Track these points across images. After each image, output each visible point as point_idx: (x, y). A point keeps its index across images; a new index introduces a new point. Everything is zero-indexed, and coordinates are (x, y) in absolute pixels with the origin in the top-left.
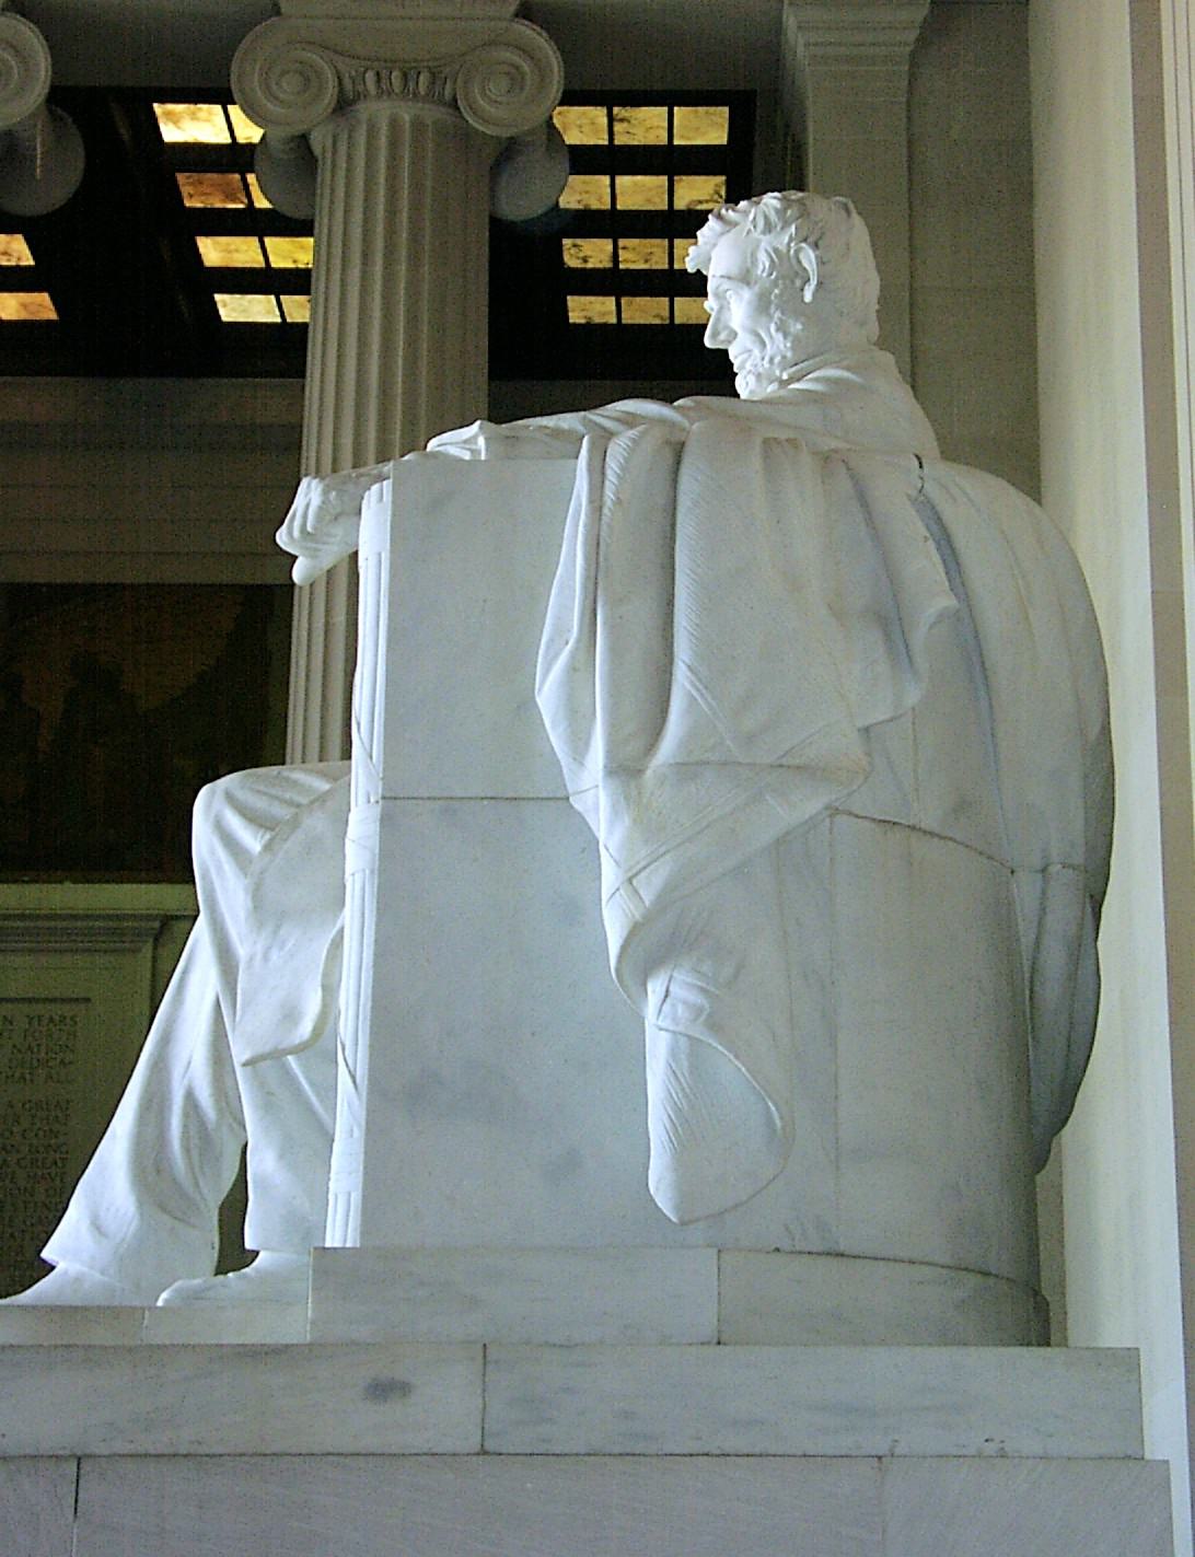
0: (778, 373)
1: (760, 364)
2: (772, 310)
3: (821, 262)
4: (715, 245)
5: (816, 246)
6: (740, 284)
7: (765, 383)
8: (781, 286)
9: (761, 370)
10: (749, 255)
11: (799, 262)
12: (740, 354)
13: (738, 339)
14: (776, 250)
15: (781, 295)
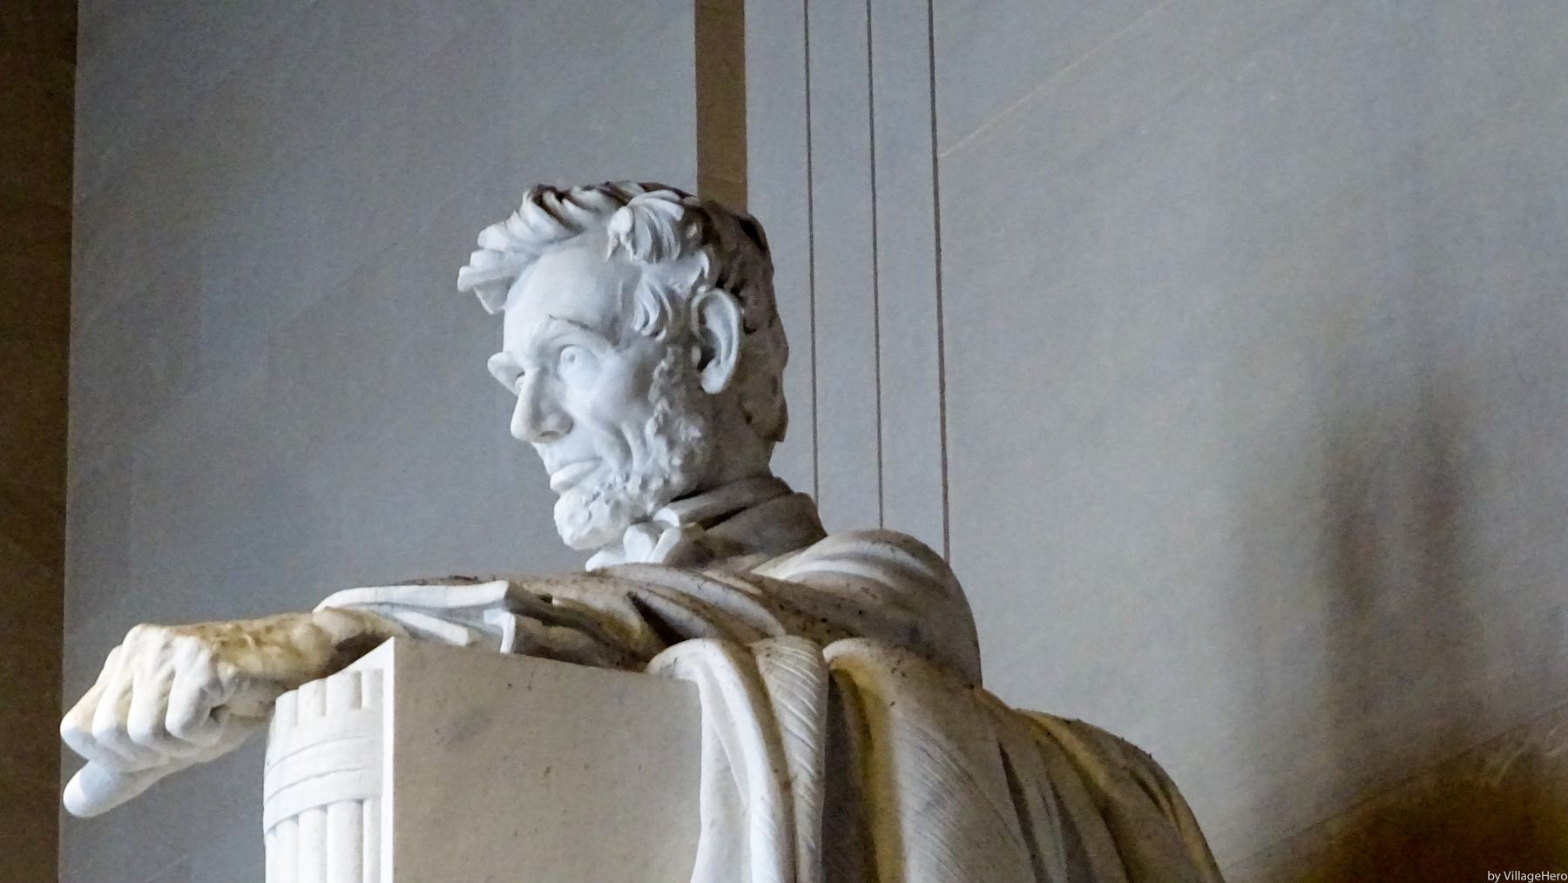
0: (650, 507)
1: (619, 487)
2: (653, 393)
3: (747, 329)
4: (534, 258)
5: (735, 292)
6: (605, 341)
7: (624, 520)
8: (671, 358)
9: (622, 497)
10: (620, 292)
11: (702, 320)
12: (577, 461)
13: (575, 433)
14: (672, 296)
15: (670, 373)
